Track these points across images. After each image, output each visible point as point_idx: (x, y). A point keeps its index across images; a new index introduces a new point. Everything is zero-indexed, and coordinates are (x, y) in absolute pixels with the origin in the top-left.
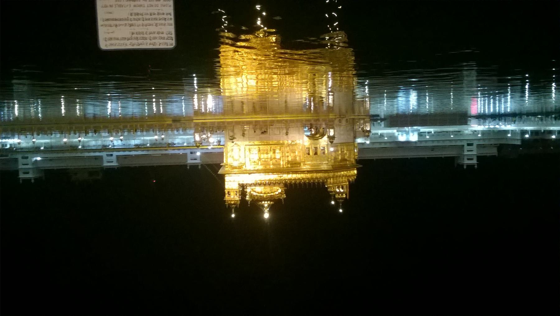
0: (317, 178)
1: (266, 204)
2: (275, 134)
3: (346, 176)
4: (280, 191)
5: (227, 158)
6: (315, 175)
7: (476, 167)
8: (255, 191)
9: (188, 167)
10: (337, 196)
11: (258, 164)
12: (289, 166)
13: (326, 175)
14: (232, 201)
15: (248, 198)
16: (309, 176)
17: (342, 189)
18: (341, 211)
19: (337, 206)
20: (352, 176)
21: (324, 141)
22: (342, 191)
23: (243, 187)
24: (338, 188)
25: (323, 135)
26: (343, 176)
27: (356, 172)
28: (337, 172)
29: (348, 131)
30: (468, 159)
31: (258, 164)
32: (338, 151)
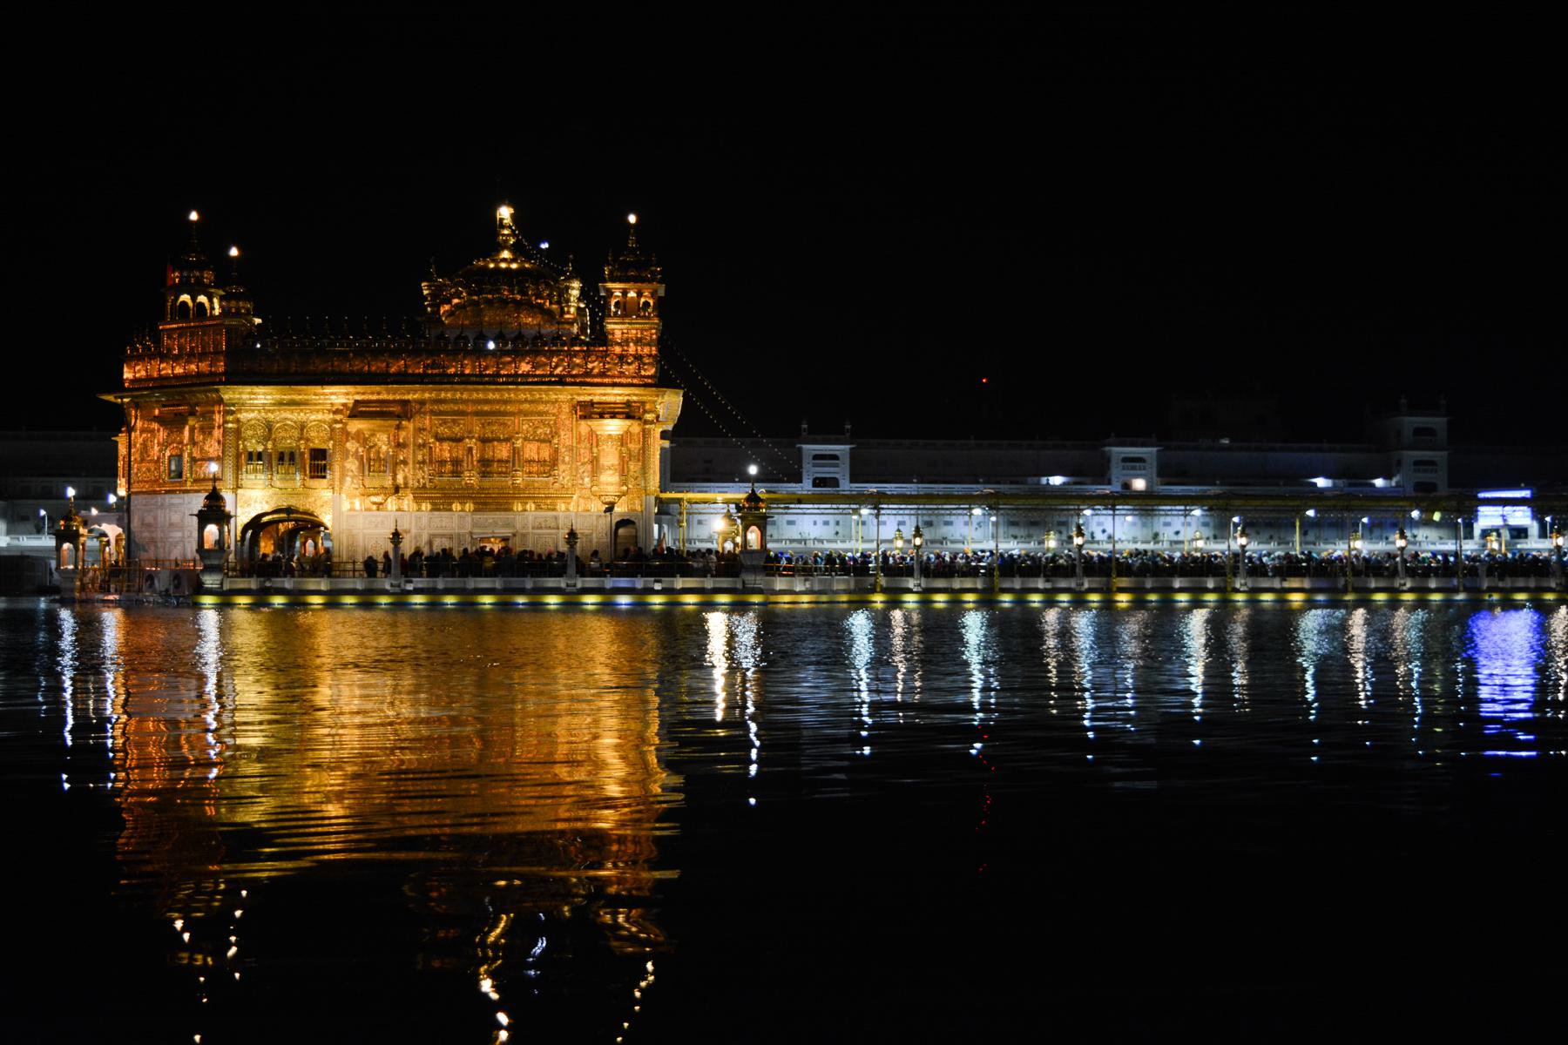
2: (451, 537)
3: (164, 357)
19: (211, 238)
20: (139, 358)
21: (253, 498)
22: (185, 298)
25: (256, 524)
26: (176, 359)
29: (153, 541)
32: (193, 460)
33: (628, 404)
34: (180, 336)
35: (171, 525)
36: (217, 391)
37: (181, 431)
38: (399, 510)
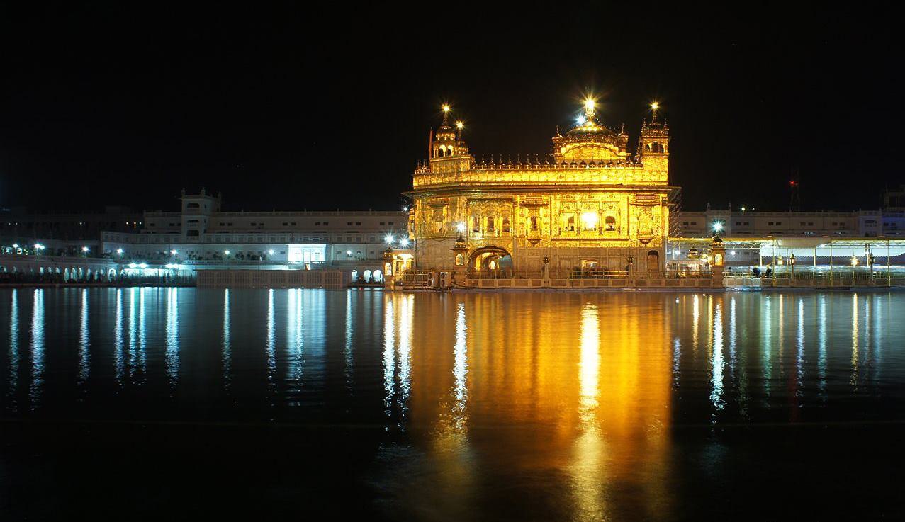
1: (591, 127)
3: (433, 175)
4: (563, 150)
7: (183, 191)
8: (611, 150)
9: (730, 206)
13: (474, 178)
17: (441, 151)
18: (446, 109)
19: (453, 118)
20: (421, 175)
23: (634, 159)
24: (449, 152)
26: (439, 175)
27: (415, 183)
30: (197, 205)
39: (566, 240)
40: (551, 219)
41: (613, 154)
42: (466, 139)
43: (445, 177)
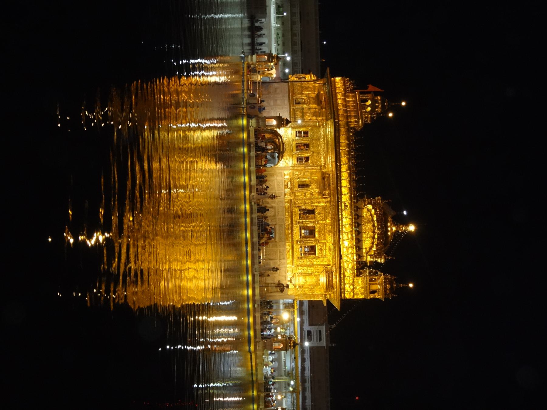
0: (348, 145)
2: (274, 216)
3: (345, 95)
4: (370, 207)
5: (314, 295)
6: (343, 149)
8: (371, 248)
10: (379, 110)
11: (325, 244)
12: (327, 192)
13: (343, 130)
14: (385, 288)
15: (381, 260)
16: (344, 159)
17: (367, 101)
19: (397, 109)
20: (344, 84)
21: (287, 134)
22: (369, 102)
23: (361, 267)
25: (278, 135)
26: (345, 100)
27: (338, 79)
28: (338, 110)
29: (269, 93)
31: (325, 244)
32: (303, 109)
33: (333, 287)
34: (353, 101)
35: (276, 100)
36: (331, 118)
37: (314, 103)
38: (285, 194)
39: (292, 212)
40: (309, 199)
41: (368, 249)
42: (379, 120)
43: (343, 105)
